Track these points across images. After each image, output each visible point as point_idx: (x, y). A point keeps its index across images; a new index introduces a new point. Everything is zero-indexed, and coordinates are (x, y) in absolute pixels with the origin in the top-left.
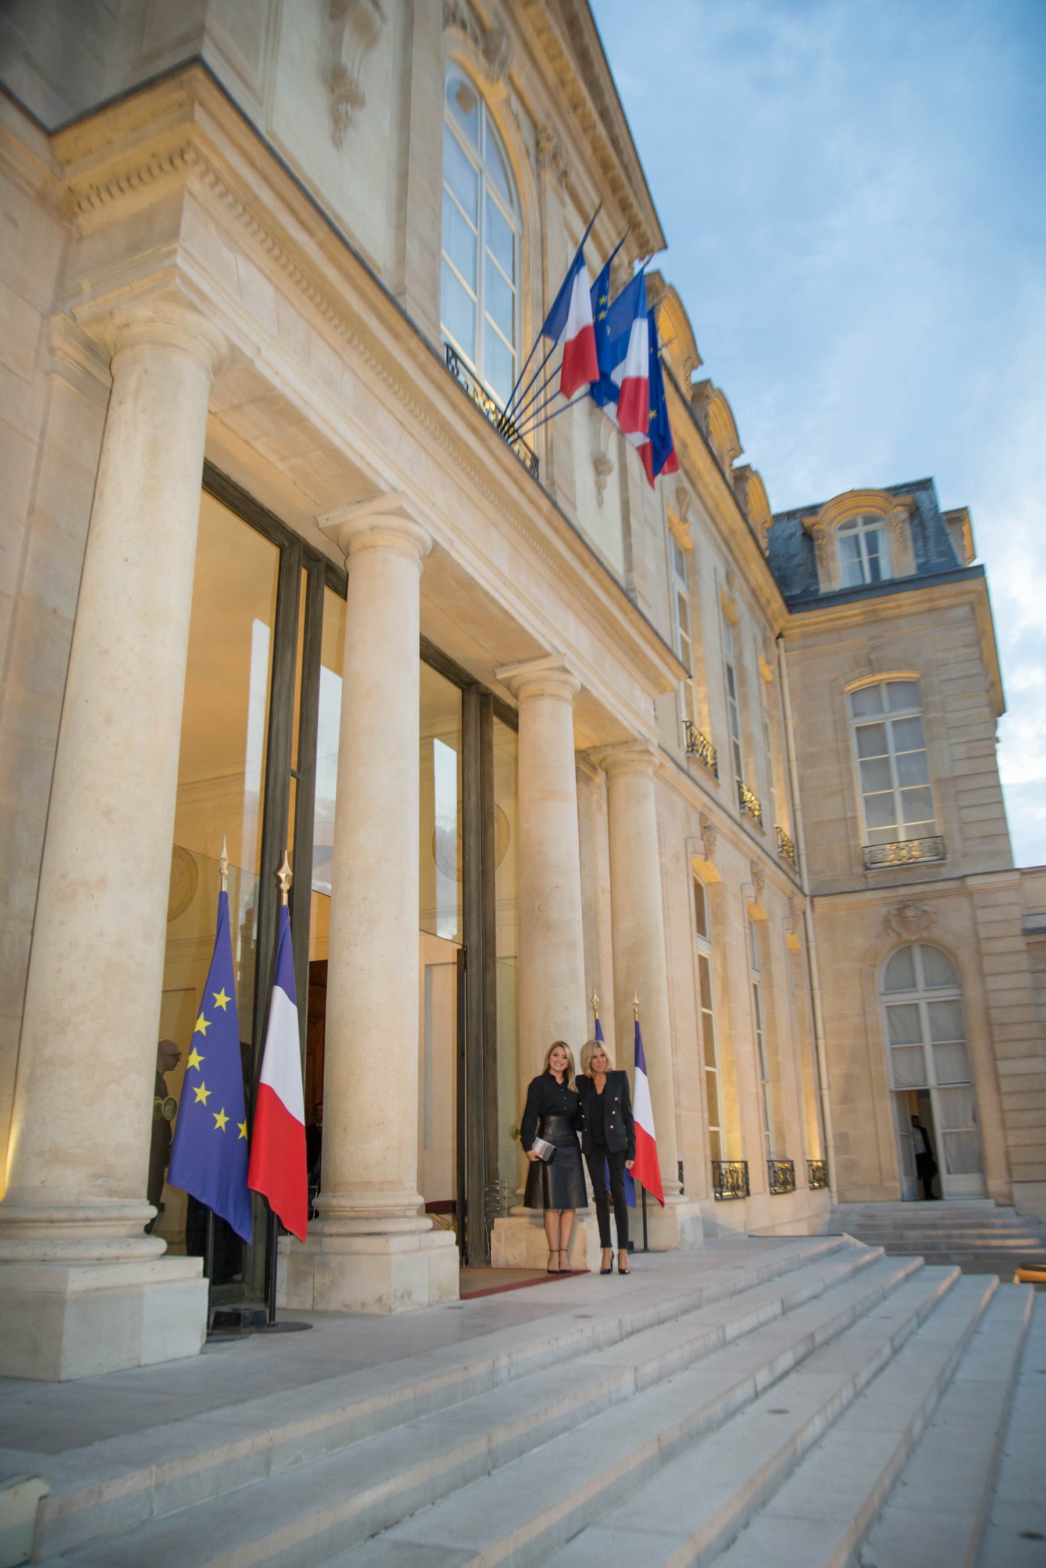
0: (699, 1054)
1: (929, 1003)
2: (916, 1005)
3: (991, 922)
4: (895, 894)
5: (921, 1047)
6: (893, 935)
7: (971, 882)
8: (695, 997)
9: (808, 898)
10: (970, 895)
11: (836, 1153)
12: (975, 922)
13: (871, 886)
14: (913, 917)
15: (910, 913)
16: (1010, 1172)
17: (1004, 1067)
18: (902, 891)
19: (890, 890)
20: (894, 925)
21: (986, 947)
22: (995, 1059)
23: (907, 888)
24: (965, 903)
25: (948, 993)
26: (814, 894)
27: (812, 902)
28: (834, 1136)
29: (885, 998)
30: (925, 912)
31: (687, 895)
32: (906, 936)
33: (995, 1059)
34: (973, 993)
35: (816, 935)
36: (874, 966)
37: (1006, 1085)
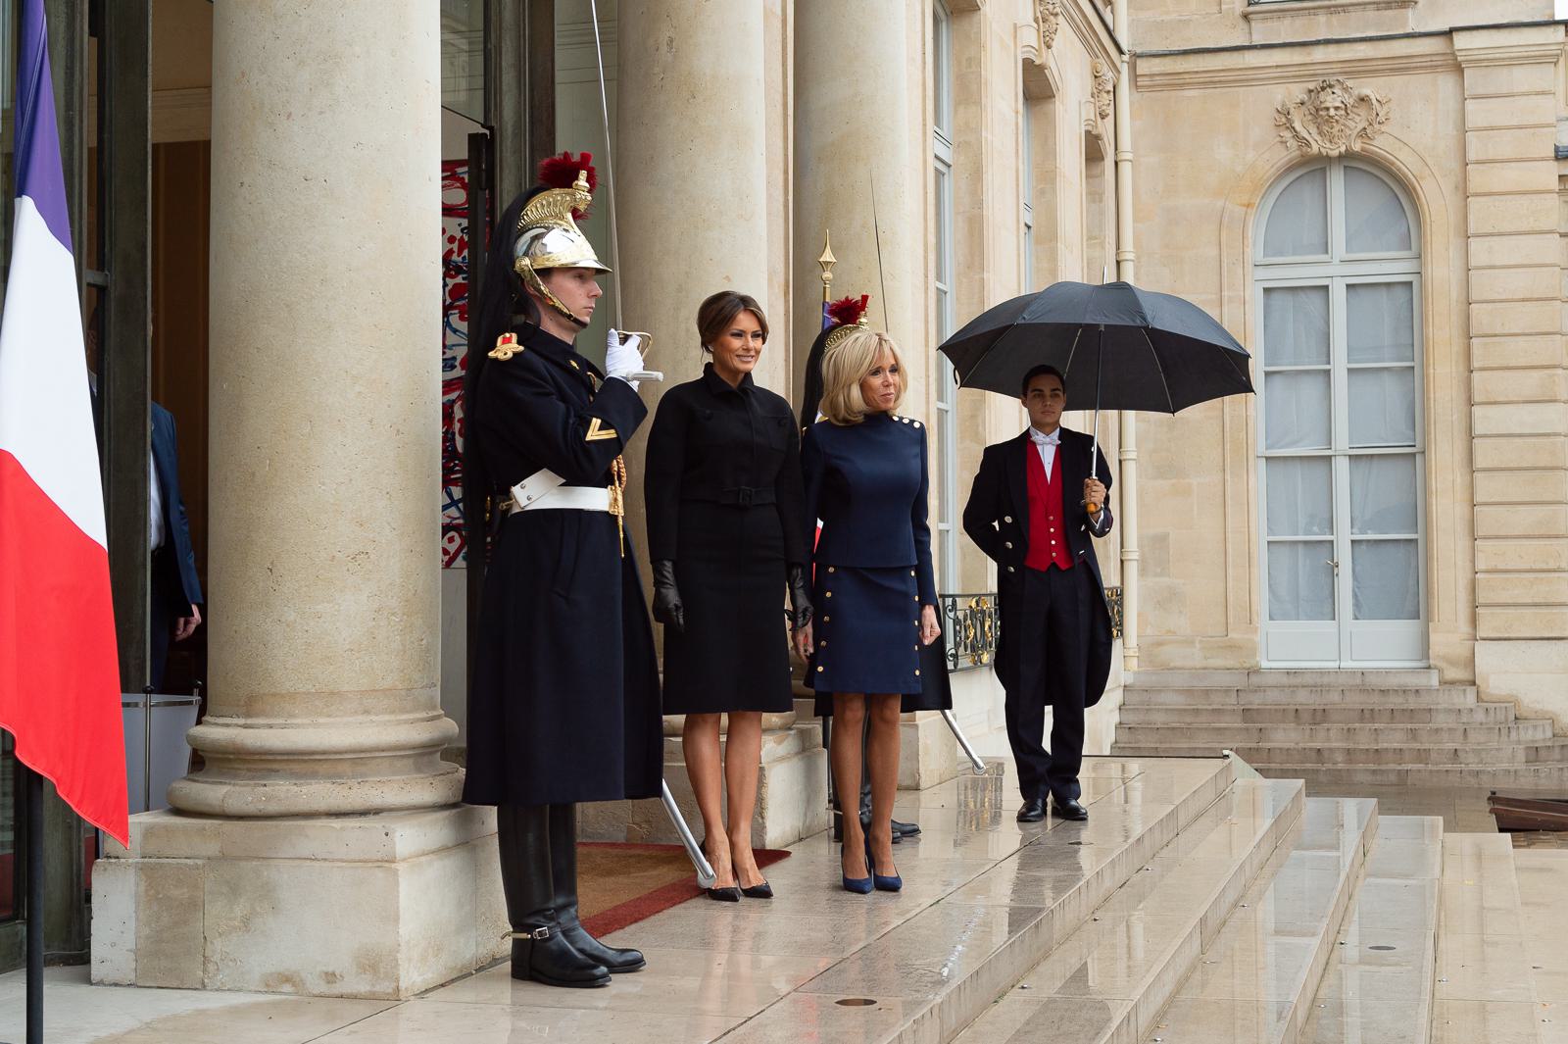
0: (928, 377)
1: (1348, 286)
2: (1326, 288)
3: (1492, 129)
4: (1308, 60)
5: (1327, 372)
6: (1292, 143)
7: (1461, 41)
8: (926, 258)
9: (1126, 58)
10: (1459, 69)
11: (1143, 571)
12: (1463, 130)
13: (1257, 40)
14: (1337, 108)
15: (1331, 100)
16: (1474, 621)
17: (1486, 419)
18: (1320, 54)
19: (1298, 50)
20: (1298, 126)
21: (1478, 179)
22: (1470, 403)
23: (1332, 48)
24: (1446, 83)
25: (1392, 267)
26: (1139, 51)
27: (1133, 67)
28: (1140, 538)
29: (1262, 273)
30: (1363, 99)
31: (920, 34)
32: (1318, 145)
33: (1470, 403)
34: (1442, 272)
35: (1136, 136)
36: (1248, 206)
37: (1484, 456)
